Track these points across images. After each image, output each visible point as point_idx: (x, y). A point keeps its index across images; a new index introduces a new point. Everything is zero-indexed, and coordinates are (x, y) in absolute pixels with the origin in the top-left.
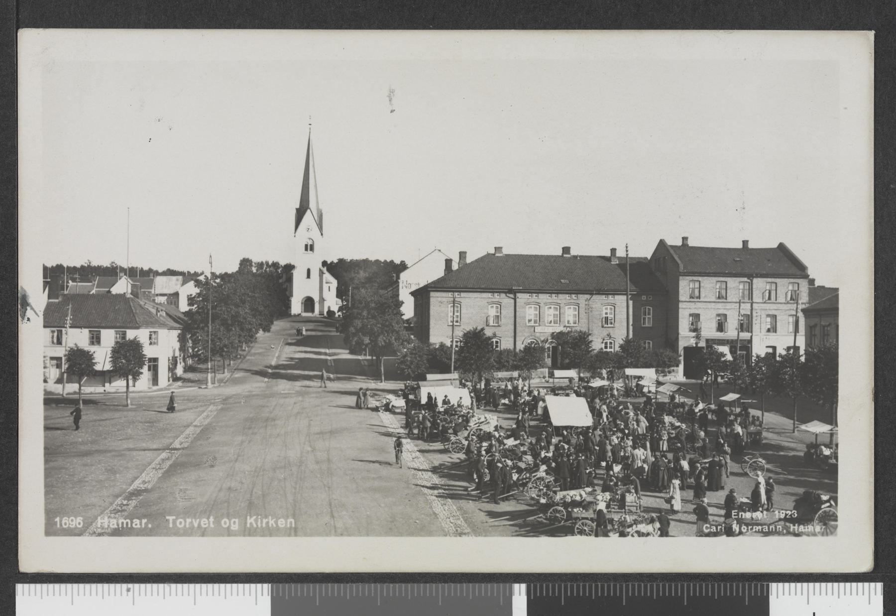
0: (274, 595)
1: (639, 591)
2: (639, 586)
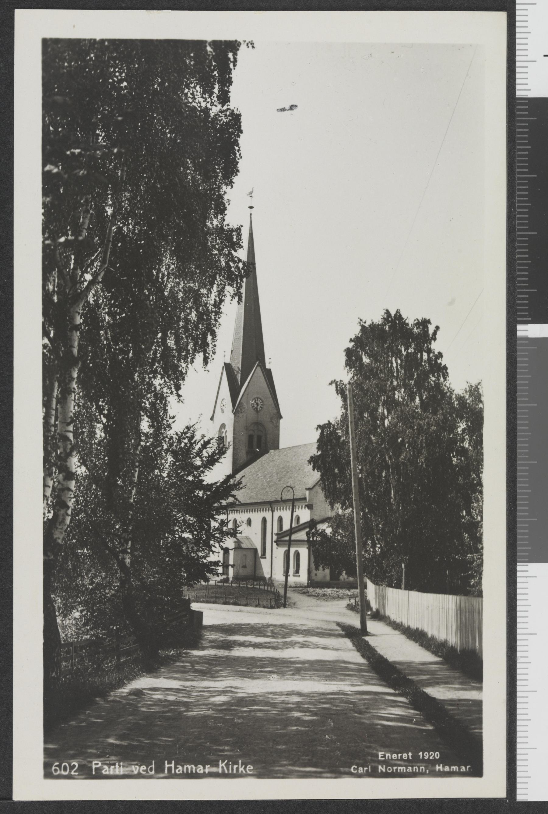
0: (527, 560)
1: (525, 259)
2: (520, 219)
